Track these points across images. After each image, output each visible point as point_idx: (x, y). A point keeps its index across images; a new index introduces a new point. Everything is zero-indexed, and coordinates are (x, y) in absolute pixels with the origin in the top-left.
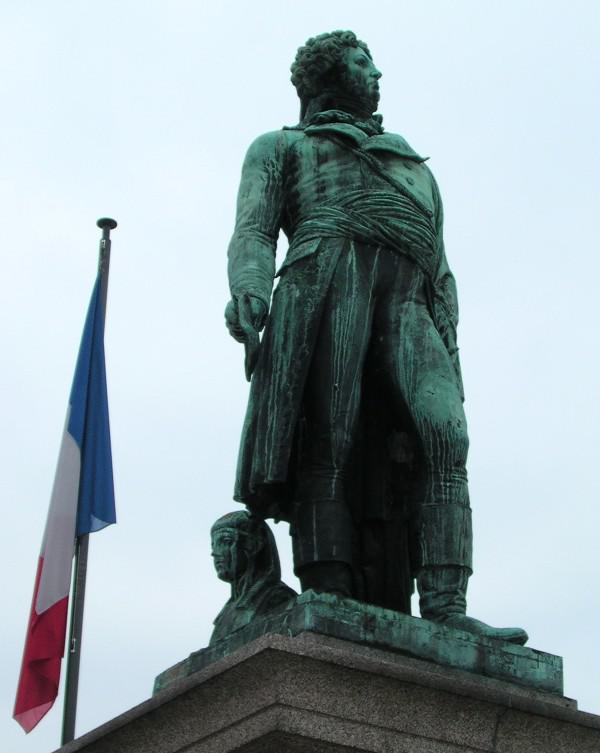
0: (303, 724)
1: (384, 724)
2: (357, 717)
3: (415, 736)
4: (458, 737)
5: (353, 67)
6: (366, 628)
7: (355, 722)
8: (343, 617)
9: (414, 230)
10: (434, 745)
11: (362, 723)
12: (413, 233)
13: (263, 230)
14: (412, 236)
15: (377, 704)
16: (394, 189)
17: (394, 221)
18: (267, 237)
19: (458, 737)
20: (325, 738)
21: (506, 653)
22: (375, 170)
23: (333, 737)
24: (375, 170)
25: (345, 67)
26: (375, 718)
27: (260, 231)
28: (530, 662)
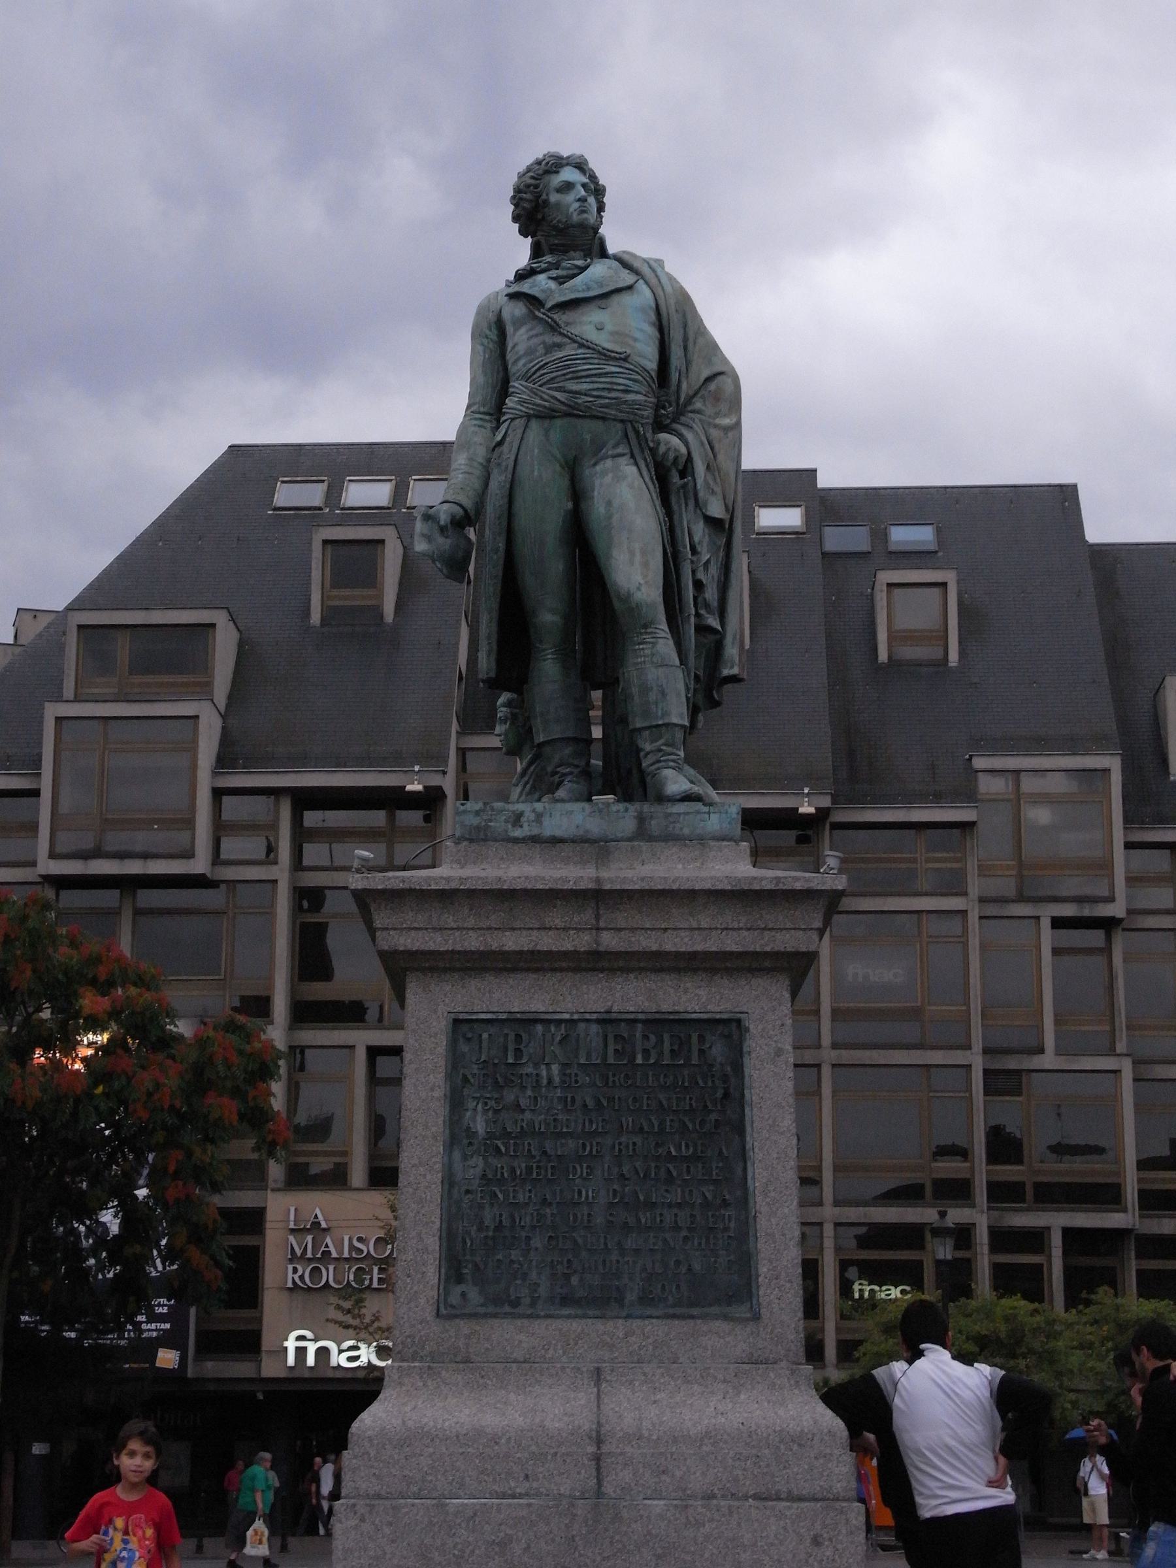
0: (402, 940)
1: (481, 925)
2: (454, 925)
3: (514, 929)
4: (557, 921)
5: (554, 198)
6: (514, 826)
7: (453, 929)
8: (491, 821)
9: (596, 386)
10: (535, 933)
11: (458, 929)
12: (598, 389)
13: (482, 409)
14: (595, 393)
15: (471, 910)
16: (576, 345)
17: (573, 386)
18: (487, 417)
19: (558, 922)
20: (423, 947)
21: (670, 814)
22: (554, 328)
23: (432, 946)
24: (554, 328)
25: (546, 203)
26: (471, 922)
27: (479, 413)
28: (699, 817)
